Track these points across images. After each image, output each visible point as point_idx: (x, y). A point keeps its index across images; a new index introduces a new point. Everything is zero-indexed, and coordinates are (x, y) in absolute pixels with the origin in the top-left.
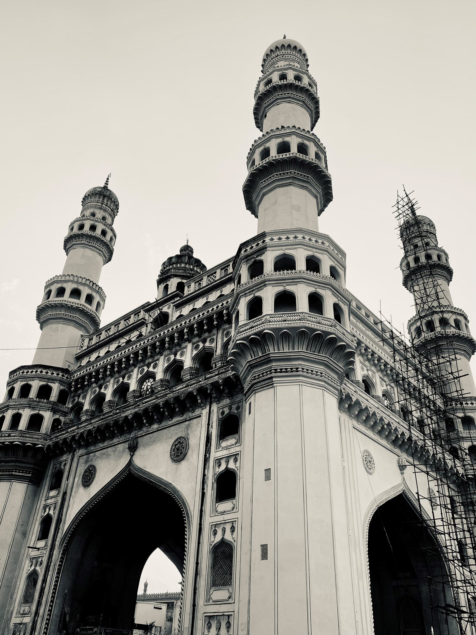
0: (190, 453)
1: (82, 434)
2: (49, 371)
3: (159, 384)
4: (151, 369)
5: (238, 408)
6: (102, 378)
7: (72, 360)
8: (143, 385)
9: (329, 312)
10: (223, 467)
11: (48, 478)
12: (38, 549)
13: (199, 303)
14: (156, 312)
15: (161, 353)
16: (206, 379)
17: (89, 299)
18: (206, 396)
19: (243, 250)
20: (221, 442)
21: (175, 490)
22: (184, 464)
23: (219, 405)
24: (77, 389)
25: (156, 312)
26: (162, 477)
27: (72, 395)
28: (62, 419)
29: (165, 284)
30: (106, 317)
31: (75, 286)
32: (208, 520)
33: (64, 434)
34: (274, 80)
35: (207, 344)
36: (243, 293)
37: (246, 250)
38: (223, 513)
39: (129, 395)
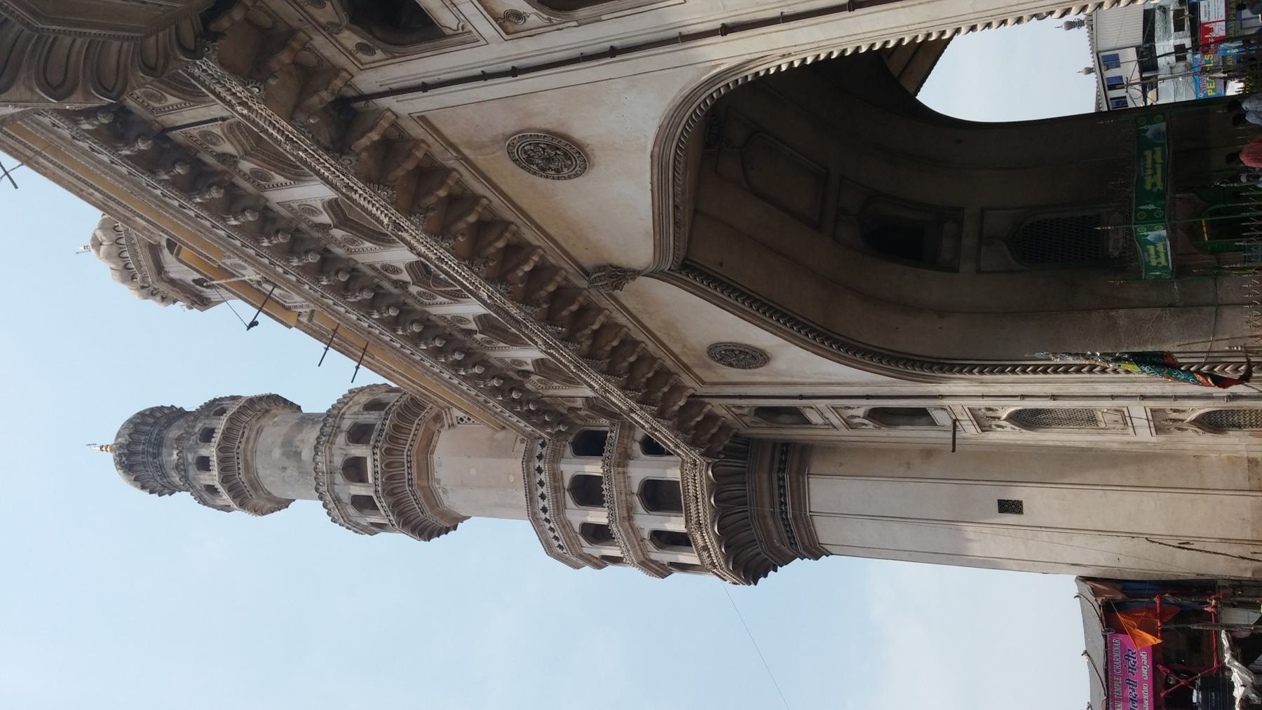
0: (539, 122)
11: (784, 432)
12: (955, 421)
20: (448, 32)
21: (663, 138)
22: (580, 130)
27: (579, 422)
28: (639, 434)
31: (339, 478)
35: (227, 148)
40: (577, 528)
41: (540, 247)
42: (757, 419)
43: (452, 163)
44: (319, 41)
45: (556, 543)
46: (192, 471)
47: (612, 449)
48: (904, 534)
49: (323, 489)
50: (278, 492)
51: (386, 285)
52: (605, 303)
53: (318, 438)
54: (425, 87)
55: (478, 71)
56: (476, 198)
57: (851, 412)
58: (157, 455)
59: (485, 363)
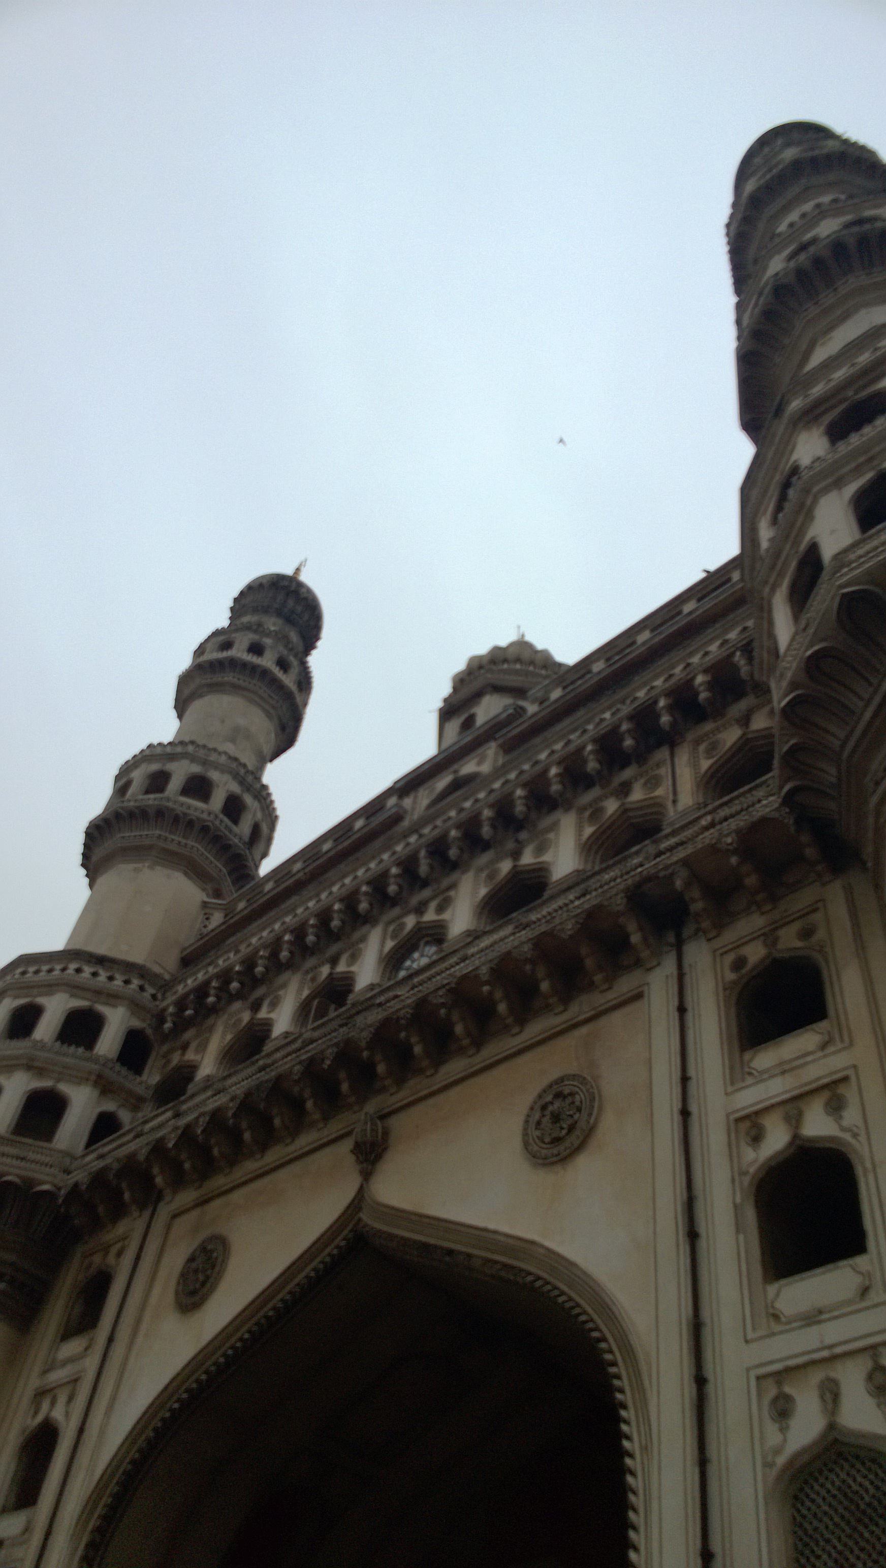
0: (608, 1123)
1: (188, 1130)
2: (101, 972)
5: (807, 933)
10: (776, 1140)
16: (660, 854)
17: (233, 808)
18: (664, 915)
23: (718, 943)
27: (165, 1048)
28: (125, 1116)
31: (196, 769)
32: (735, 1360)
33: (129, 1142)
35: (637, 795)
36: (830, 480)
38: (813, 1318)
40: (41, 1000)
41: (436, 1071)
44: (757, 922)
47: (122, 1076)
49: (190, 748)
50: (196, 707)
51: (426, 893)
52: (335, 1127)
53: (245, 766)
54: (682, 1010)
55: (691, 1072)
56: (522, 1022)
57: (62, 1399)
58: (279, 613)
59: (290, 966)
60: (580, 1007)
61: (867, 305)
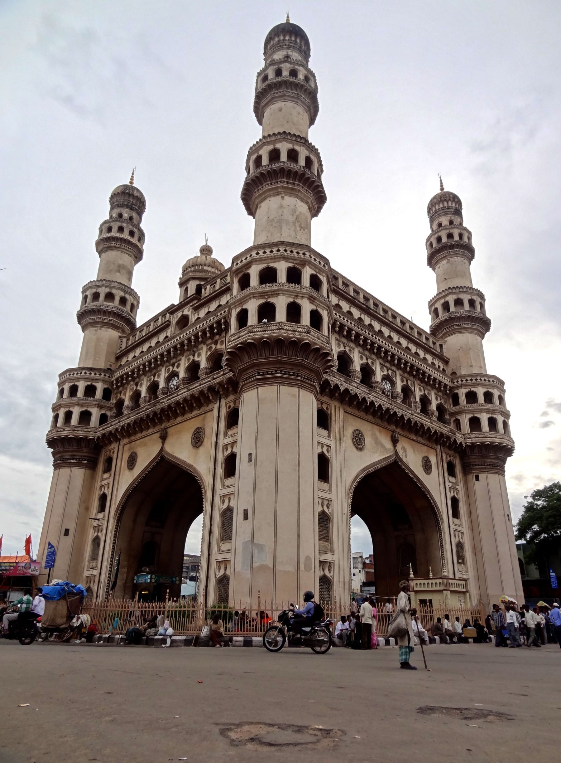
0: (205, 440)
1: (123, 427)
3: (181, 382)
4: (175, 369)
6: (137, 377)
7: (113, 359)
8: (169, 382)
9: (306, 319)
10: (229, 451)
12: (99, 520)
13: (213, 306)
14: (179, 314)
15: (182, 354)
16: (214, 379)
17: (123, 301)
19: (235, 264)
22: (202, 449)
24: (118, 387)
25: (179, 314)
26: (185, 460)
27: (115, 392)
28: (108, 413)
29: (185, 287)
30: (142, 317)
31: (108, 290)
32: (219, 492)
34: (270, 77)
35: (219, 346)
37: (237, 264)
38: (228, 487)
39: (159, 392)
40: (77, 383)
42: (107, 456)
43: (201, 410)
45: (72, 373)
46: (119, 224)
47: (105, 403)
48: (61, 498)
52: (156, 429)
53: (124, 285)
54: (219, 417)
57: (106, 488)
58: (127, 206)
60: (203, 410)
61: (270, 196)
